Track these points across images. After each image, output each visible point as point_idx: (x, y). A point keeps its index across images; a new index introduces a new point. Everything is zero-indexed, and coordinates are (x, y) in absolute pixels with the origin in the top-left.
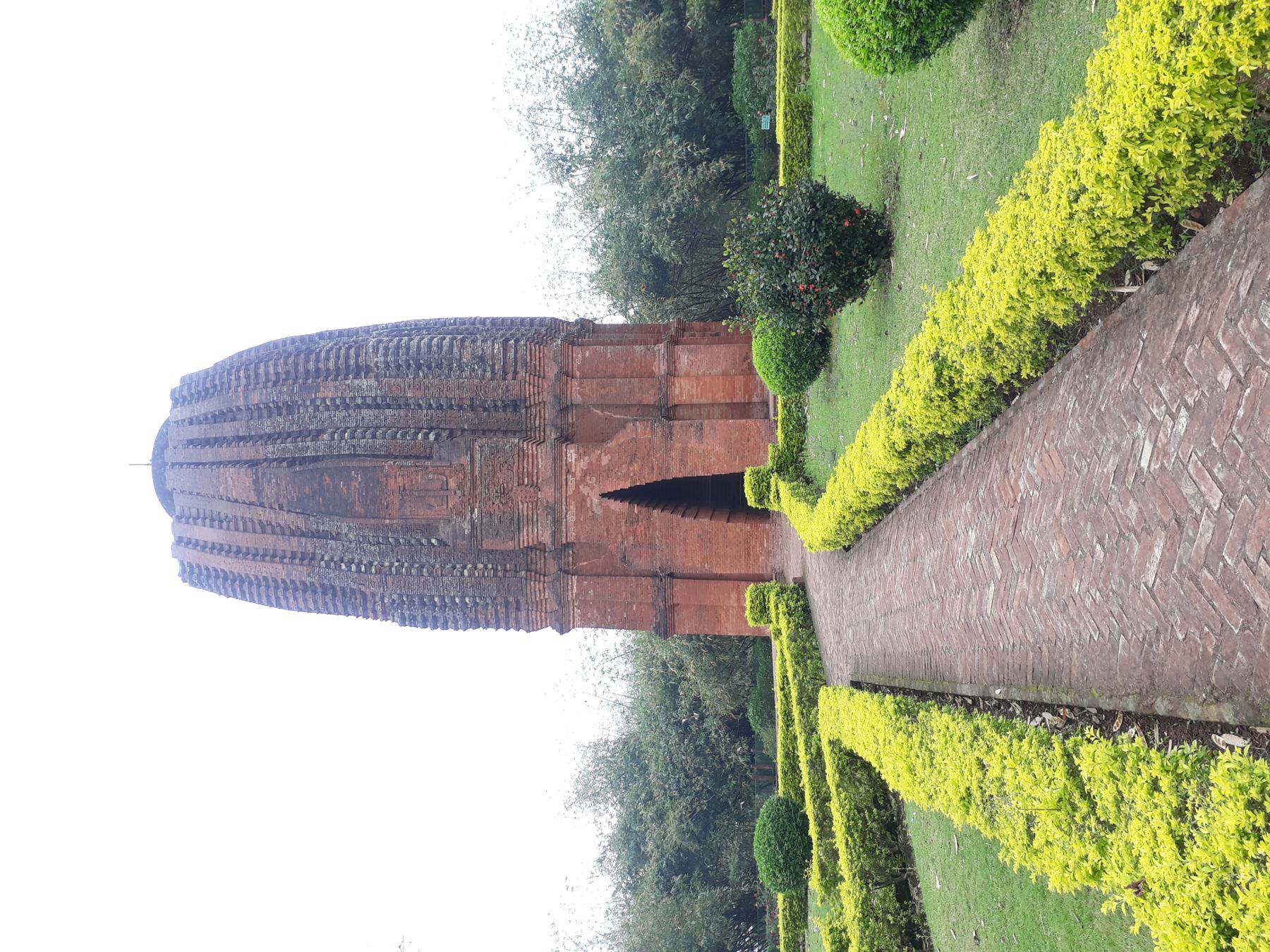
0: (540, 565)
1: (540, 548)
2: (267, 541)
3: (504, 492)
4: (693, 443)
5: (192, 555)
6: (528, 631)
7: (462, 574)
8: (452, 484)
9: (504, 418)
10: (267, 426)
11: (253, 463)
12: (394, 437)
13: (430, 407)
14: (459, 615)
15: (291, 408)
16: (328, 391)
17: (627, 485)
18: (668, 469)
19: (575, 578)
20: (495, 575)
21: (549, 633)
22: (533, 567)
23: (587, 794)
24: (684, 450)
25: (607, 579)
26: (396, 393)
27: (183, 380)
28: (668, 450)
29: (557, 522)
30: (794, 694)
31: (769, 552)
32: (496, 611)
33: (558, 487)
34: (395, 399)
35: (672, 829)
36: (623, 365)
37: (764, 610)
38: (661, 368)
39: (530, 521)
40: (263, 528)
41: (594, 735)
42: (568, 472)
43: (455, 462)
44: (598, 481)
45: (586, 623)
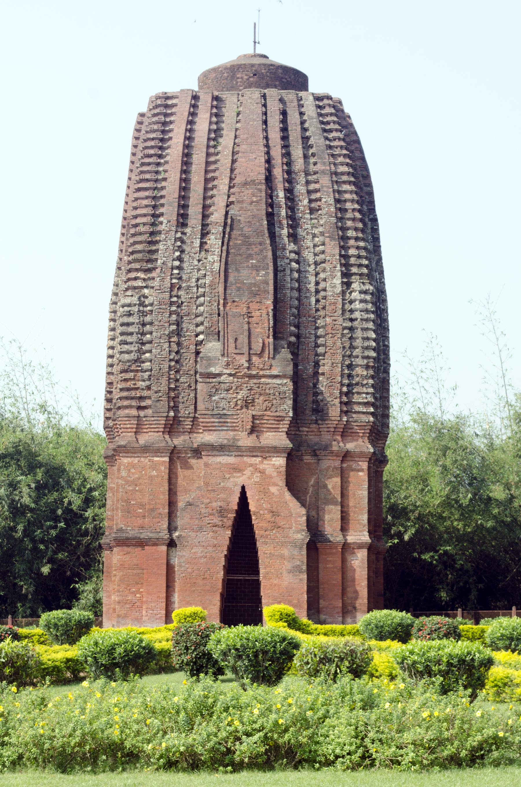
4: (288, 565)
10: (300, 189)
11: (269, 179)
19: (167, 459)
25: (167, 488)
33: (253, 451)
44: (256, 483)
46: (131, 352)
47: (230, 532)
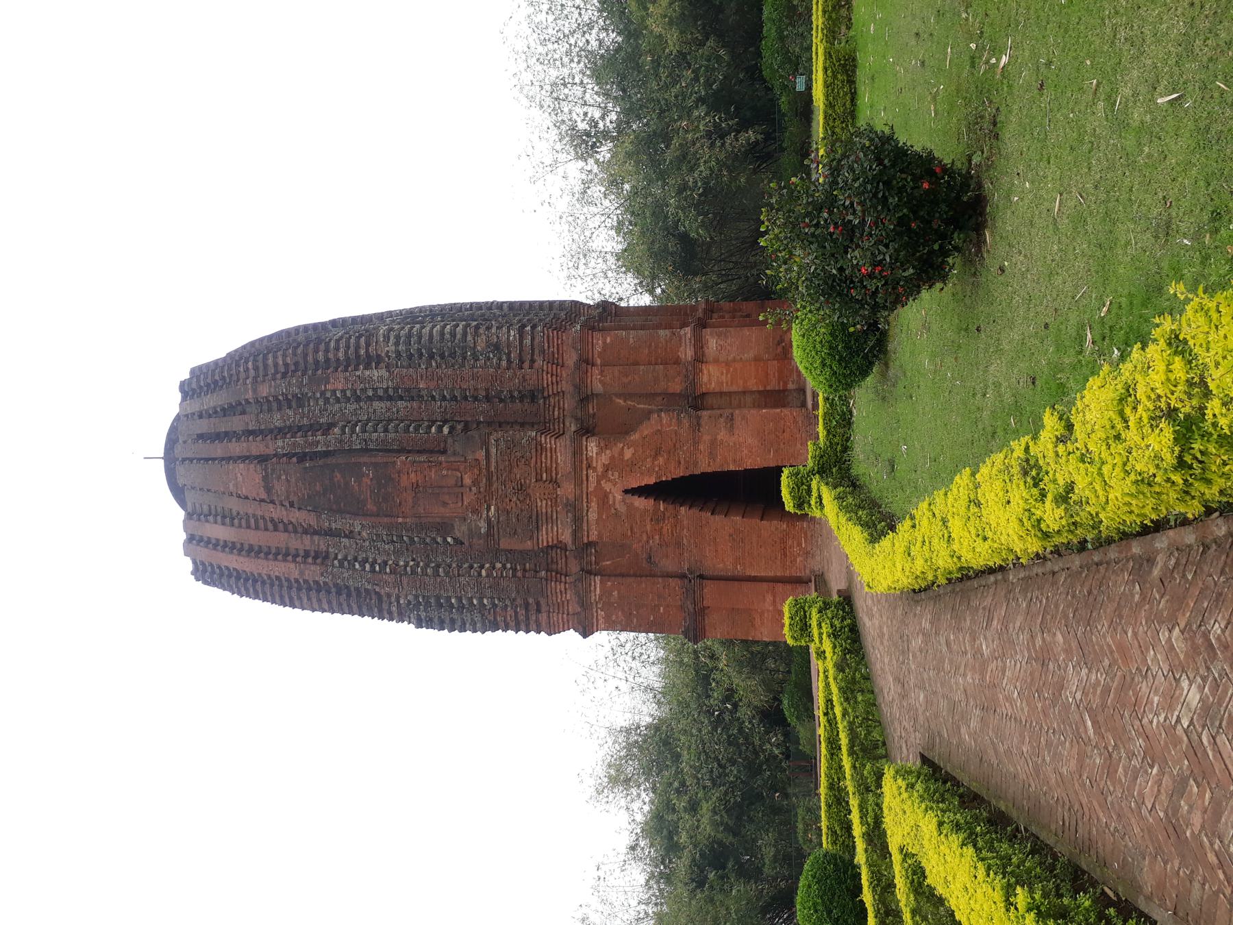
0: (561, 564)
1: (560, 546)
2: (279, 539)
3: (521, 489)
4: (722, 435)
5: (205, 554)
6: (550, 634)
7: (480, 574)
8: (467, 481)
10: (277, 420)
11: (262, 459)
12: (407, 430)
13: (444, 398)
14: (477, 618)
15: (300, 401)
16: (338, 383)
17: (652, 481)
18: (696, 464)
19: (598, 579)
20: (514, 576)
21: (571, 636)
22: (554, 567)
23: (618, 779)
24: (713, 442)
26: (408, 384)
27: (193, 371)
28: (696, 443)
29: (578, 520)
30: (844, 741)
31: (808, 553)
32: (516, 613)
33: (578, 482)
34: (408, 390)
35: (705, 820)
36: (646, 351)
37: (804, 628)
38: (687, 353)
39: (549, 519)
40: (276, 525)
41: (623, 721)
42: (589, 466)
43: (470, 457)
45: (611, 626)
46: (472, 620)
47: (683, 509)
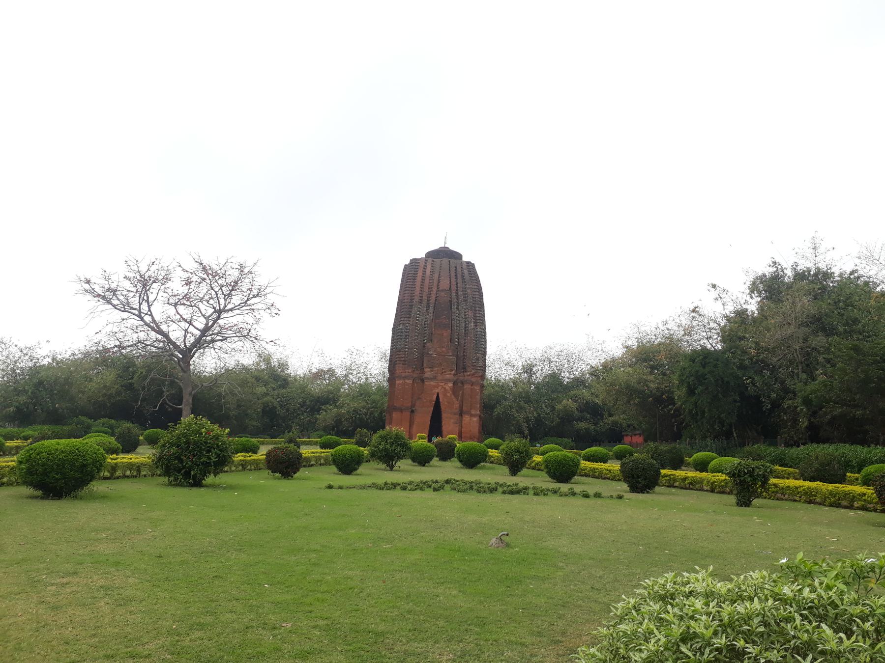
2: (426, 289)
4: (452, 421)
9: (461, 367)
10: (460, 293)
16: (471, 314)
29: (431, 379)
38: (473, 412)
40: (430, 289)
